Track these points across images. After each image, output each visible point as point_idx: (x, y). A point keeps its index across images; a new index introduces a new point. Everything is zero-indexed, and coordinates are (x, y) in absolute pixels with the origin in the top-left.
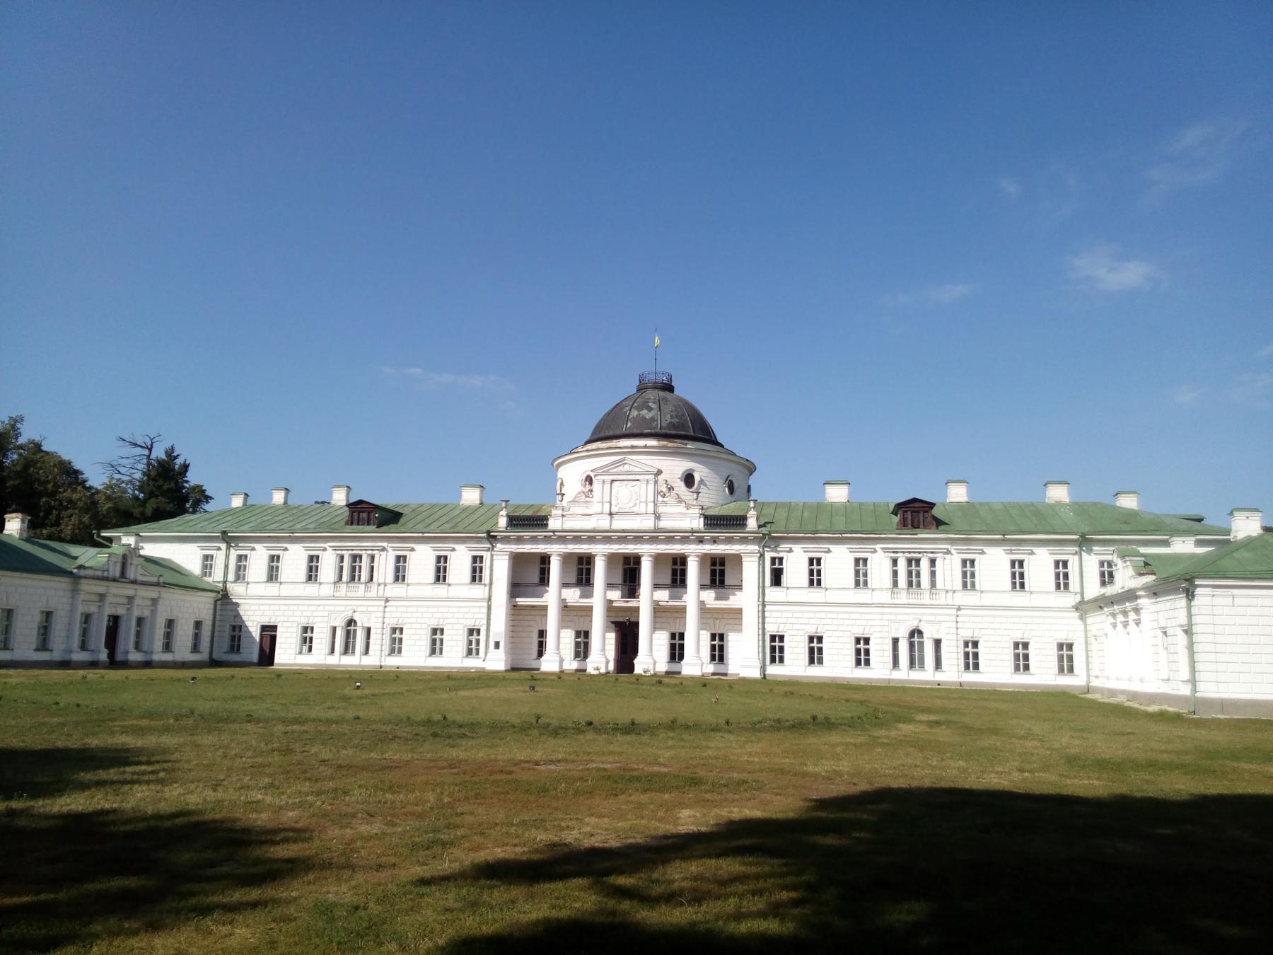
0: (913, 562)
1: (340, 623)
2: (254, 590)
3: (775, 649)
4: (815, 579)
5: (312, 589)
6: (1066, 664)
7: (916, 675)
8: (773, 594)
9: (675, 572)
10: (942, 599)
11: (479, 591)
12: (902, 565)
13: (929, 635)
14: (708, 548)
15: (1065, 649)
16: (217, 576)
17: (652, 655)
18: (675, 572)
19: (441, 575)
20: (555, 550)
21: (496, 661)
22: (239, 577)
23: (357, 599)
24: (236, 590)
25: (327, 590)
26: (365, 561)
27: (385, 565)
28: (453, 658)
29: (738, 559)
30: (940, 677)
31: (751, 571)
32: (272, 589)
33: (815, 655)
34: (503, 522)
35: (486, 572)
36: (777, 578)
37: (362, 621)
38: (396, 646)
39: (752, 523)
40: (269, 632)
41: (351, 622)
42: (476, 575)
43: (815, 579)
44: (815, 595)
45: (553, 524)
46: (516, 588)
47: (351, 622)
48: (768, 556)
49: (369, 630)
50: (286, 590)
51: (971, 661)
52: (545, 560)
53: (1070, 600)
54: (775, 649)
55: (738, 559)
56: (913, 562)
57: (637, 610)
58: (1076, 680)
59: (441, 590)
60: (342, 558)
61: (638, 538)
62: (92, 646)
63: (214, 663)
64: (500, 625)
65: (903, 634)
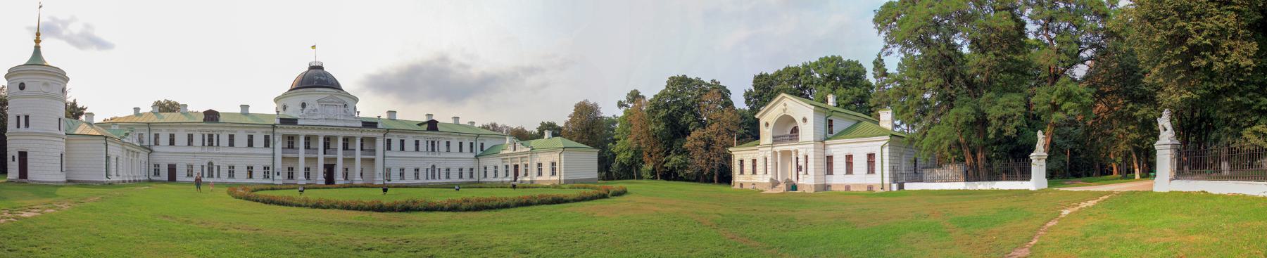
0: (433, 143)
1: (206, 164)
3: (387, 173)
5: (190, 149)
8: (388, 153)
11: (269, 151)
14: (365, 134)
16: (146, 143)
17: (339, 178)
19: (250, 144)
21: (279, 180)
22: (156, 143)
24: (155, 148)
25: (199, 150)
27: (224, 140)
28: (258, 178)
29: (373, 140)
31: (380, 145)
32: (172, 149)
33: (402, 175)
34: (278, 122)
37: (215, 164)
38: (231, 173)
39: (379, 126)
40: (172, 169)
41: (210, 164)
42: (267, 145)
44: (402, 154)
45: (300, 122)
47: (210, 164)
54: (387, 173)
55: (373, 140)
58: (475, 179)
59: (250, 150)
61: (339, 128)
63: (150, 181)
64: (279, 164)
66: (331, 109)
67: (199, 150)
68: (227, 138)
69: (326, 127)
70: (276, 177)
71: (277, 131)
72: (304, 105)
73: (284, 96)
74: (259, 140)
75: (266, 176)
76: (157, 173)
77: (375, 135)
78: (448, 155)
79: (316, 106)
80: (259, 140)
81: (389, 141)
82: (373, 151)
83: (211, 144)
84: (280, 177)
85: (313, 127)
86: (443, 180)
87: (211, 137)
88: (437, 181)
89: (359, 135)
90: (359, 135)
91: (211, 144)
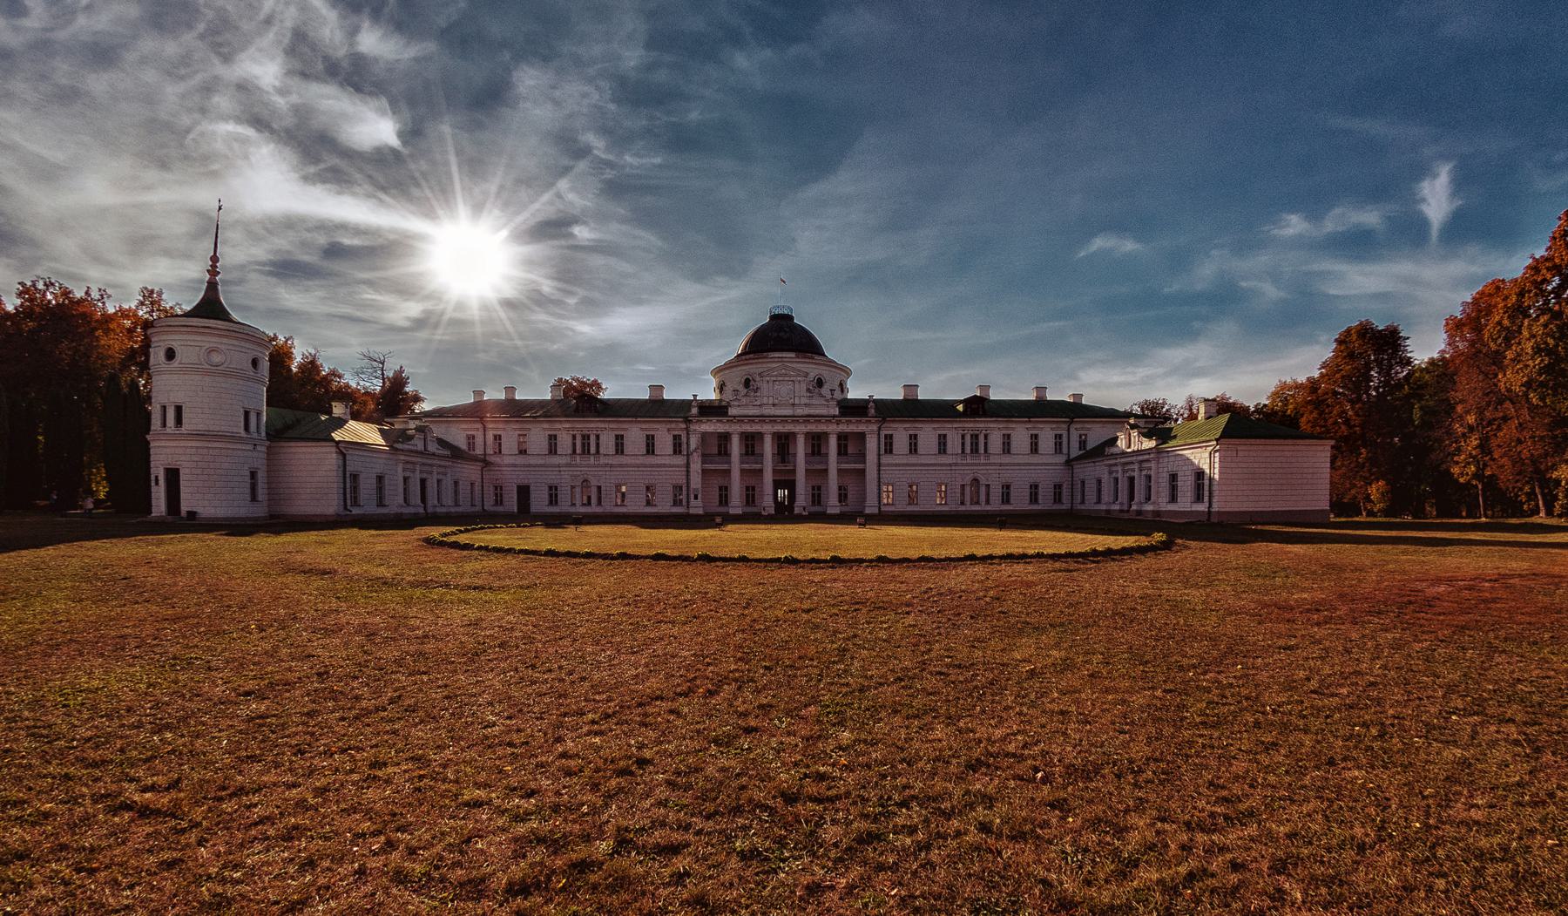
2: (507, 460)
4: (913, 448)
6: (1058, 498)
7: (976, 508)
8: (886, 459)
9: (817, 443)
10: (992, 460)
11: (680, 460)
12: (968, 438)
13: (983, 481)
14: (843, 428)
15: (1058, 487)
16: (479, 451)
18: (817, 443)
20: (735, 429)
23: (589, 466)
26: (593, 438)
30: (988, 508)
31: (872, 444)
34: (694, 411)
35: (684, 446)
36: (889, 450)
40: (524, 492)
42: (677, 449)
43: (913, 448)
44: (913, 459)
45: (732, 411)
46: (705, 458)
48: (883, 433)
49: (599, 488)
50: (533, 461)
51: (1006, 498)
52: (725, 438)
53: (1063, 459)
55: (861, 437)
56: (975, 437)
57: (794, 471)
58: (1066, 506)
59: (651, 460)
60: (574, 437)
61: (794, 419)
62: (412, 502)
64: (696, 481)
65: (968, 480)
66: (784, 389)
67: (563, 460)
68: (612, 442)
69: (773, 419)
70: (693, 502)
71: (692, 427)
72: (747, 383)
73: (728, 366)
74: (664, 442)
75: (677, 503)
76: (499, 500)
77: (862, 428)
78: (1006, 459)
79: (784, 390)
80: (664, 442)
81: (889, 438)
82: (862, 456)
83: (586, 450)
84: (699, 502)
85: (751, 419)
86: (996, 505)
87: (586, 437)
88: (982, 507)
89: (833, 429)
90: (833, 429)
91: (586, 450)
